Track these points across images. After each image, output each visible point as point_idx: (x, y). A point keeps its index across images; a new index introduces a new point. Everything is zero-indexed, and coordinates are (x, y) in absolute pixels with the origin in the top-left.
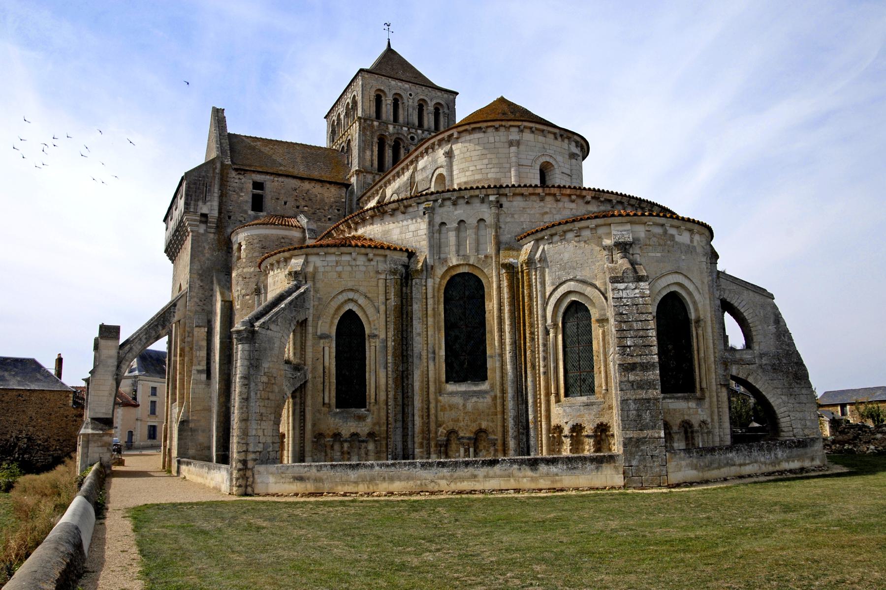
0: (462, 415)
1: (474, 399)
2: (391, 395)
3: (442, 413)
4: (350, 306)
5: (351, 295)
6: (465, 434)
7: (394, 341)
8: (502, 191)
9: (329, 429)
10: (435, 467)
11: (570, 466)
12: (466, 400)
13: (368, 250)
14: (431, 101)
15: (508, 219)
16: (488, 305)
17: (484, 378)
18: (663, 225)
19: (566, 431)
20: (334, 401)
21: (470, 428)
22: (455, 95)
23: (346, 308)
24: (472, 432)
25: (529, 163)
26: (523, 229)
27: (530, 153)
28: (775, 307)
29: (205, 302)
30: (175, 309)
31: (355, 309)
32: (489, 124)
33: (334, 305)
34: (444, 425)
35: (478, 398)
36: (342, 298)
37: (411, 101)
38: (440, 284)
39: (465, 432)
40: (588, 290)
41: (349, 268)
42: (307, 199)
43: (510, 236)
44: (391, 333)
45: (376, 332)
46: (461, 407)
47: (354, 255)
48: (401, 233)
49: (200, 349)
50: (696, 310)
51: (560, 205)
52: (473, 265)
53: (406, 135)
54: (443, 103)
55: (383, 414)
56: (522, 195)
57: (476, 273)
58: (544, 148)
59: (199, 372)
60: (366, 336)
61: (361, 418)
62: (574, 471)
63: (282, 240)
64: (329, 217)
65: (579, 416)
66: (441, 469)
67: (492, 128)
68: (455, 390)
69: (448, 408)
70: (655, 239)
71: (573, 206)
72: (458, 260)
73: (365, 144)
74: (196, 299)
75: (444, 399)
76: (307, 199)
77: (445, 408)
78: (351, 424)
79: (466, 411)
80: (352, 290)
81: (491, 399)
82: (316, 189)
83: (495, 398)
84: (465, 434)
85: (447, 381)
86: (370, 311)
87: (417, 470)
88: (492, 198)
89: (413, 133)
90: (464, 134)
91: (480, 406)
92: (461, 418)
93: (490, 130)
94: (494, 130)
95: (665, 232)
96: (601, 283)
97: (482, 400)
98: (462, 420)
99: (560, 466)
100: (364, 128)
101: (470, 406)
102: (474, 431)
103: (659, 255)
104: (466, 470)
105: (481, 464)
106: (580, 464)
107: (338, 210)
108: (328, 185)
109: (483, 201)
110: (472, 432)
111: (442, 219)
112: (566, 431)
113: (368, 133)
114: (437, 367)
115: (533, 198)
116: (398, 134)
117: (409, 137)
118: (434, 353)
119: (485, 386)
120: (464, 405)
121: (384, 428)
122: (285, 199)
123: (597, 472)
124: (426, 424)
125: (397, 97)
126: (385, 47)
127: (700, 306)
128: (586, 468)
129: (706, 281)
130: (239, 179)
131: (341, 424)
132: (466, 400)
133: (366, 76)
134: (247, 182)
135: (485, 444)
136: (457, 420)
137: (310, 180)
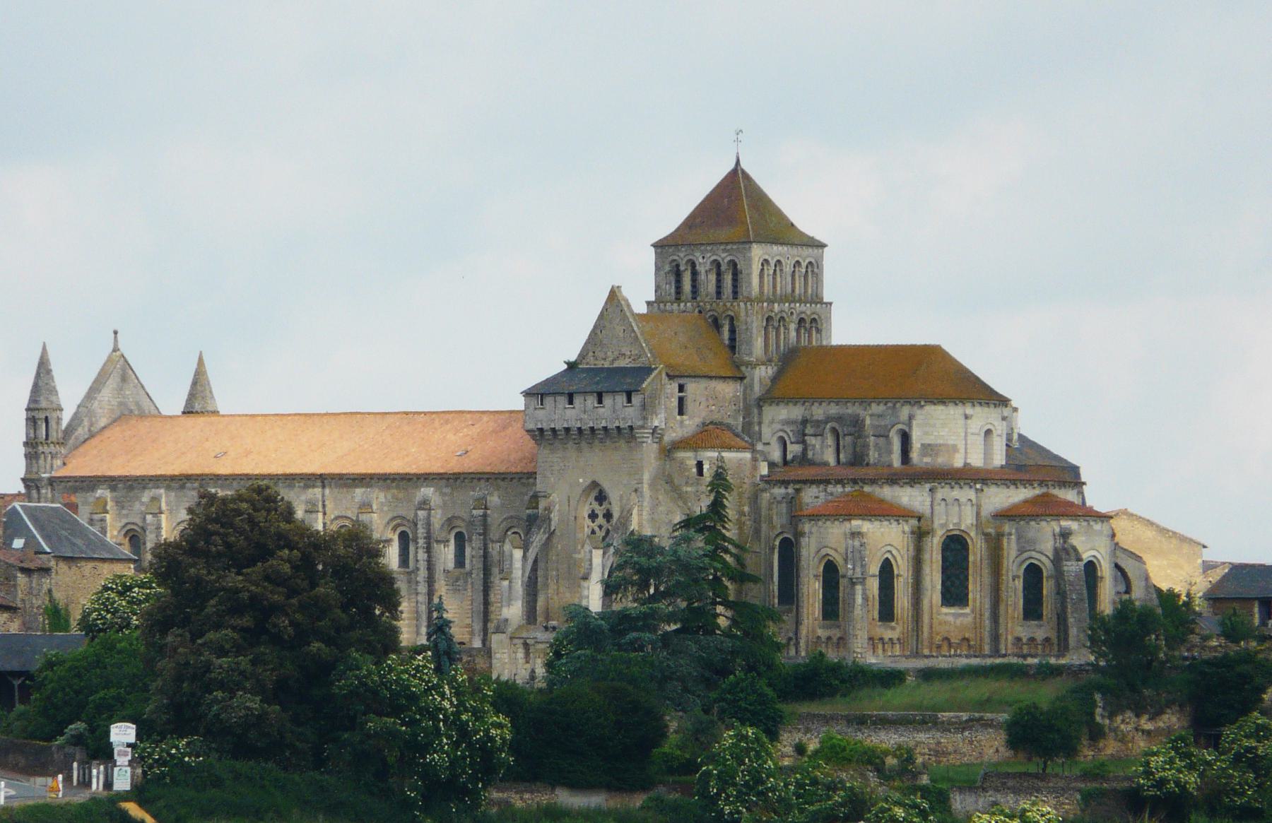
1: (961, 619)
2: (910, 614)
5: (889, 548)
17: (968, 605)
19: (1024, 640)
23: (885, 556)
25: (977, 431)
28: (1146, 570)
33: (879, 554)
36: (884, 550)
40: (1044, 559)
47: (892, 521)
50: (1101, 570)
51: (1019, 490)
52: (963, 531)
54: (813, 261)
57: (964, 535)
61: (893, 629)
75: (941, 617)
83: (975, 618)
86: (899, 559)
109: (971, 487)
112: (1024, 640)
114: (937, 598)
119: (967, 610)
124: (931, 633)
126: (732, 166)
127: (1103, 568)
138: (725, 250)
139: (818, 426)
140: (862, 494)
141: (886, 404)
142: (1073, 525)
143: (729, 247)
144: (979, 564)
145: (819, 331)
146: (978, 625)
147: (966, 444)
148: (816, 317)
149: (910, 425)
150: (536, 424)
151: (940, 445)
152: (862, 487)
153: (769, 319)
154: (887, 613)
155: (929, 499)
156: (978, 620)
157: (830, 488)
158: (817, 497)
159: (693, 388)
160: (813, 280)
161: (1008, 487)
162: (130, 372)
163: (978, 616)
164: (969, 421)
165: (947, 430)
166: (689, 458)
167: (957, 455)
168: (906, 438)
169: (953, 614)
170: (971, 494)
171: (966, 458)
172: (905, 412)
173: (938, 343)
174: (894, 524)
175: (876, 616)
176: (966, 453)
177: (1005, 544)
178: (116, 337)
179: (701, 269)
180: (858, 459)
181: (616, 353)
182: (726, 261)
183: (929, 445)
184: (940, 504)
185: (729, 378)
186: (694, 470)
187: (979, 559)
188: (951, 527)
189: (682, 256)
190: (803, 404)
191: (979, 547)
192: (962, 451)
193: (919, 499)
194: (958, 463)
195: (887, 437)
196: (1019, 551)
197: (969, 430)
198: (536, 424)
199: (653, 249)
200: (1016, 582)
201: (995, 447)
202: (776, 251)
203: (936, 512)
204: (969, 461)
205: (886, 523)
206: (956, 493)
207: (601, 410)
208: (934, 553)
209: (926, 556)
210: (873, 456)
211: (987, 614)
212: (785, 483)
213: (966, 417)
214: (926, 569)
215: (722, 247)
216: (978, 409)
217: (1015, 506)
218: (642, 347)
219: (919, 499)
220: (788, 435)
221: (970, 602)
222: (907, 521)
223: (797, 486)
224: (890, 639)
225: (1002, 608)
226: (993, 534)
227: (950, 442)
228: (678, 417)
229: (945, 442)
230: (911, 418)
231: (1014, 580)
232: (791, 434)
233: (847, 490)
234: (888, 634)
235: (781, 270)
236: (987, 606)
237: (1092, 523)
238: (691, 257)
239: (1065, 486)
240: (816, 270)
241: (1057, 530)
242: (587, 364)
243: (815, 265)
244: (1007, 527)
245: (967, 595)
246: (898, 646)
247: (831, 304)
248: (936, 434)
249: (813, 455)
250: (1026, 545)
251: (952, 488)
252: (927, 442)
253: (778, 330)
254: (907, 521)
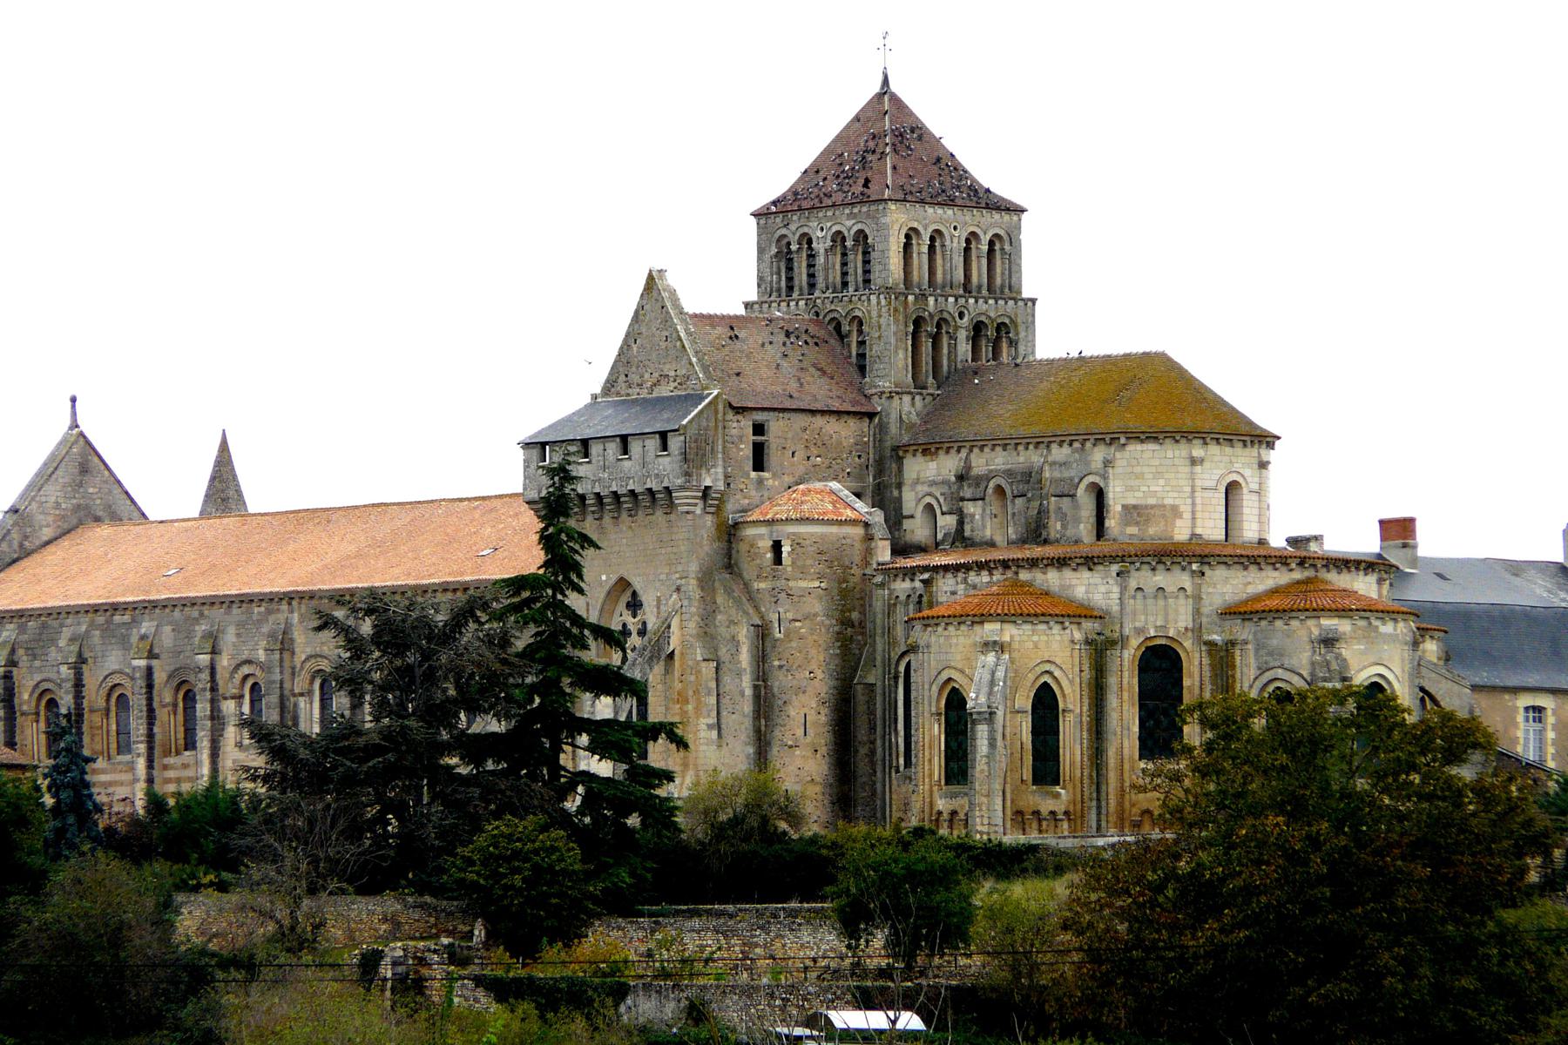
4: (1046, 678)
5: (1047, 667)
8: (1206, 560)
14: (985, 234)
15: (1210, 590)
18: (1368, 618)
25: (1212, 484)
27: (1215, 471)
29: (707, 622)
30: (669, 632)
31: (1050, 680)
32: (1168, 435)
33: (1031, 677)
36: (1039, 670)
37: (955, 240)
38: (1134, 656)
41: (1045, 638)
42: (819, 443)
44: (1085, 709)
47: (1052, 623)
48: (1087, 592)
49: (709, 694)
51: (1264, 574)
54: (1002, 233)
56: (1226, 563)
57: (1174, 645)
58: (1231, 462)
59: (710, 727)
63: (844, 542)
64: (848, 470)
70: (1360, 632)
71: (1276, 574)
72: (1156, 631)
74: (696, 618)
76: (819, 443)
80: (1049, 661)
82: (831, 426)
85: (1140, 759)
86: (1065, 683)
88: (1195, 567)
90: (1132, 441)
93: (1167, 441)
95: (1370, 624)
103: (1362, 647)
107: (859, 457)
108: (846, 417)
109: (1184, 569)
115: (1238, 566)
118: (1129, 729)
121: (1079, 806)
122: (793, 449)
124: (1120, 804)
126: (876, 88)
129: (1406, 669)
130: (738, 421)
133: (893, 207)
134: (746, 424)
137: (823, 412)
138: (851, 216)
139: (978, 485)
140: (1017, 584)
141: (1071, 445)
142: (1343, 626)
143: (856, 210)
145: (1013, 343)
147: (1194, 504)
148: (1007, 321)
149: (1105, 477)
150: (540, 492)
151: (1152, 507)
152: (1017, 573)
153: (918, 322)
154: (1046, 768)
155: (1116, 589)
157: (973, 577)
158: (954, 593)
159: (777, 427)
160: (1003, 263)
161: (1246, 568)
162: (96, 459)
164: (1198, 469)
165: (1162, 482)
166: (761, 536)
167: (1179, 523)
168: (1100, 495)
170: (1185, 580)
171: (1194, 526)
172: (1098, 455)
173: (1160, 349)
174: (1056, 629)
175: (1028, 775)
176: (1194, 518)
177: (1238, 659)
178: (73, 407)
179: (820, 247)
180: (1035, 532)
181: (656, 375)
182: (852, 232)
183: (1135, 507)
184: (1134, 597)
185: (848, 413)
186: (769, 555)
187: (1197, 684)
188: (1152, 633)
189: (793, 232)
190: (959, 451)
191: (1197, 663)
192: (1187, 516)
193: (1103, 589)
194: (1181, 533)
195: (1073, 496)
196: (1259, 668)
197: (1199, 483)
198: (540, 492)
199: (753, 220)
201: (1246, 511)
202: (932, 217)
203: (1128, 609)
204: (1199, 531)
205: (1042, 627)
206: (1160, 578)
207: (627, 464)
208: (1126, 674)
209: (1112, 681)
210: (1055, 527)
212: (910, 573)
213: (1194, 462)
214: (1112, 701)
215: (847, 211)
216: (1214, 449)
217: (1257, 598)
218: (691, 364)
219: (1103, 589)
220: (939, 502)
222: (1079, 624)
223: (926, 576)
224: (1053, 813)
227: (1168, 501)
228: (753, 474)
229: (1160, 503)
230: (1107, 463)
232: (942, 500)
233: (995, 578)
234: (1046, 806)
235: (943, 246)
237: (1376, 623)
238: (806, 230)
239: (1349, 569)
240: (1007, 247)
241: (1316, 632)
242: (618, 394)
243: (1005, 237)
244: (1243, 631)
246: (1065, 825)
247: (1034, 301)
248: (1145, 489)
249: (972, 531)
250: (1269, 658)
251: (1154, 569)
252: (1132, 501)
253: (936, 339)
254: (1079, 624)
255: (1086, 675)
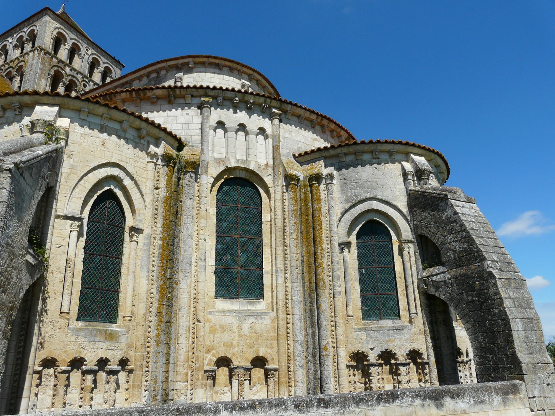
0: (237, 338)
1: (252, 320)
3: (212, 335)
5: (115, 172)
6: (239, 362)
7: (162, 239)
9: (66, 352)
10: (315, 407)
11: (476, 399)
12: (241, 320)
13: (144, 125)
15: (287, 135)
16: (266, 216)
17: (262, 297)
20: (75, 309)
21: (246, 355)
22: (122, 67)
24: (248, 360)
26: (299, 147)
32: (227, 63)
34: (214, 351)
35: (256, 319)
39: (239, 360)
43: (288, 151)
44: (159, 229)
45: (141, 226)
46: (235, 329)
53: (80, 80)
55: (140, 332)
60: (127, 229)
61: (112, 337)
62: (483, 406)
65: (388, 341)
66: (324, 410)
67: (227, 68)
68: (226, 308)
69: (220, 330)
73: (42, 73)
77: (216, 329)
78: (101, 345)
79: (241, 334)
81: (270, 320)
84: (239, 362)
87: (289, 413)
89: (86, 82)
91: (258, 328)
92: (235, 343)
94: (229, 71)
96: (403, 205)
97: (260, 321)
98: (236, 345)
99: (466, 399)
100: (43, 58)
101: (247, 328)
102: (251, 358)
104: (357, 410)
105: (377, 400)
106: (487, 396)
110: (248, 360)
111: (220, 118)
113: (46, 64)
116: (73, 76)
117: (82, 83)
119: (261, 305)
120: (239, 326)
123: (505, 406)
125: (75, 47)
128: (493, 401)
131: (86, 344)
132: (241, 320)
135: (259, 375)
136: (229, 345)
144: (279, 224)
146: (283, 332)
156: (282, 323)
163: (282, 316)
169: (238, 313)
200: (346, 253)
209: (188, 203)
211: (298, 311)
221: (267, 292)
225: (325, 300)
226: (302, 179)
231: (342, 250)
236: (298, 296)
245: (261, 277)
255: (163, 193)
